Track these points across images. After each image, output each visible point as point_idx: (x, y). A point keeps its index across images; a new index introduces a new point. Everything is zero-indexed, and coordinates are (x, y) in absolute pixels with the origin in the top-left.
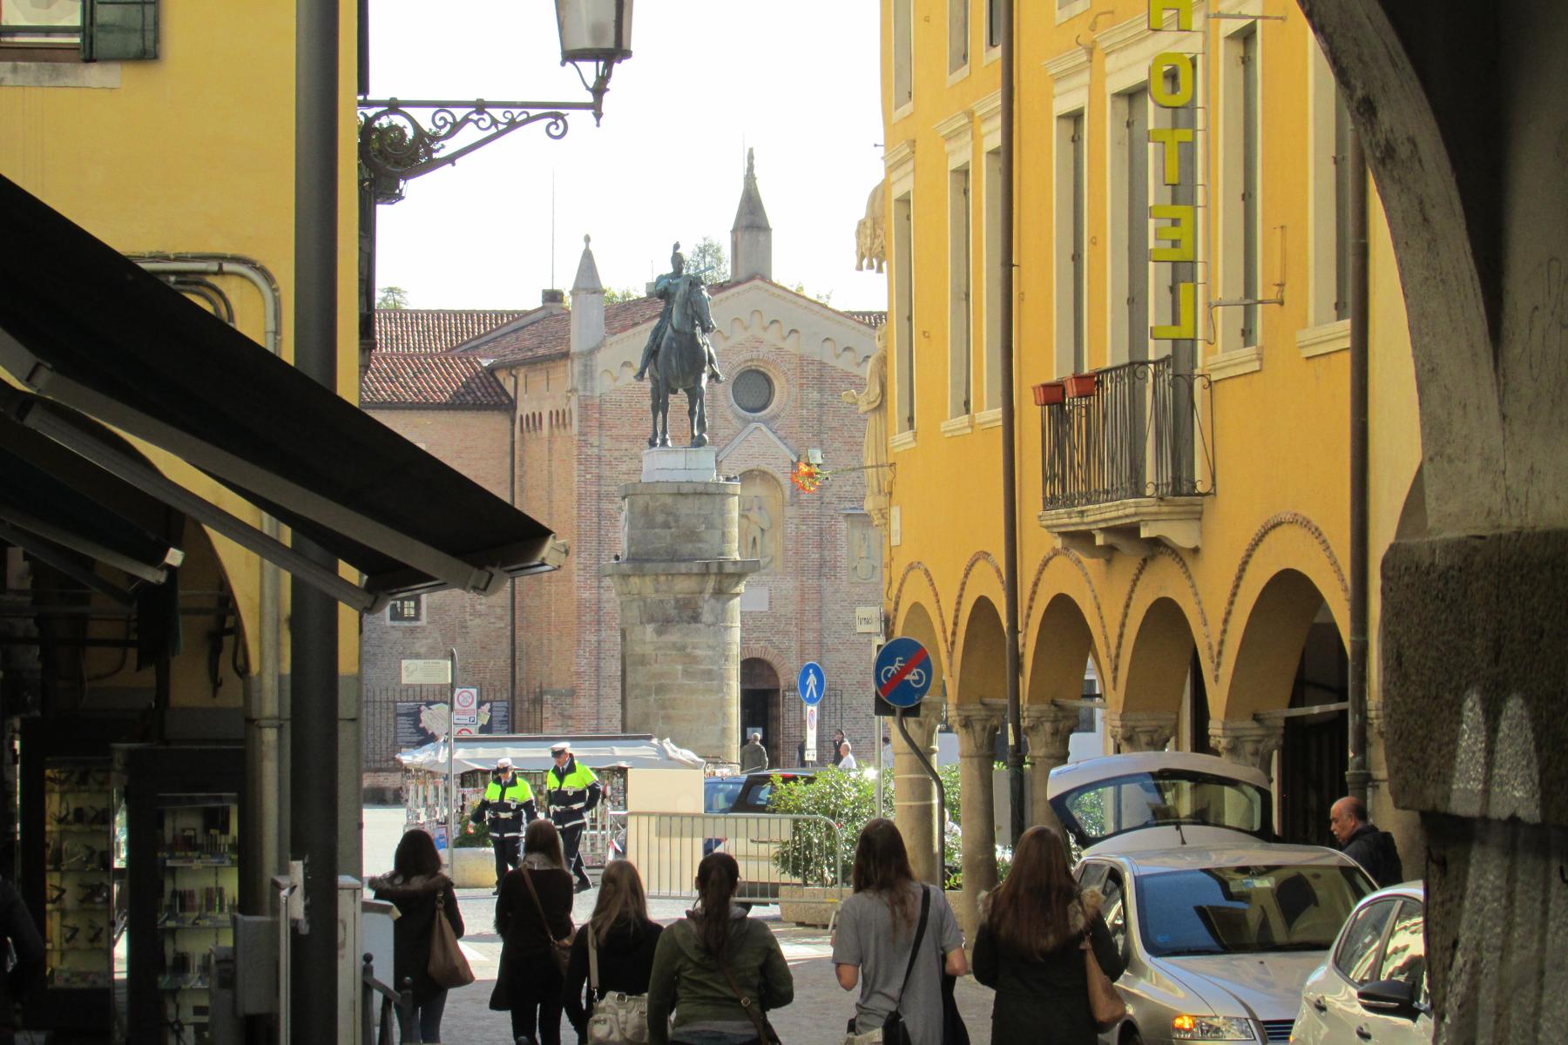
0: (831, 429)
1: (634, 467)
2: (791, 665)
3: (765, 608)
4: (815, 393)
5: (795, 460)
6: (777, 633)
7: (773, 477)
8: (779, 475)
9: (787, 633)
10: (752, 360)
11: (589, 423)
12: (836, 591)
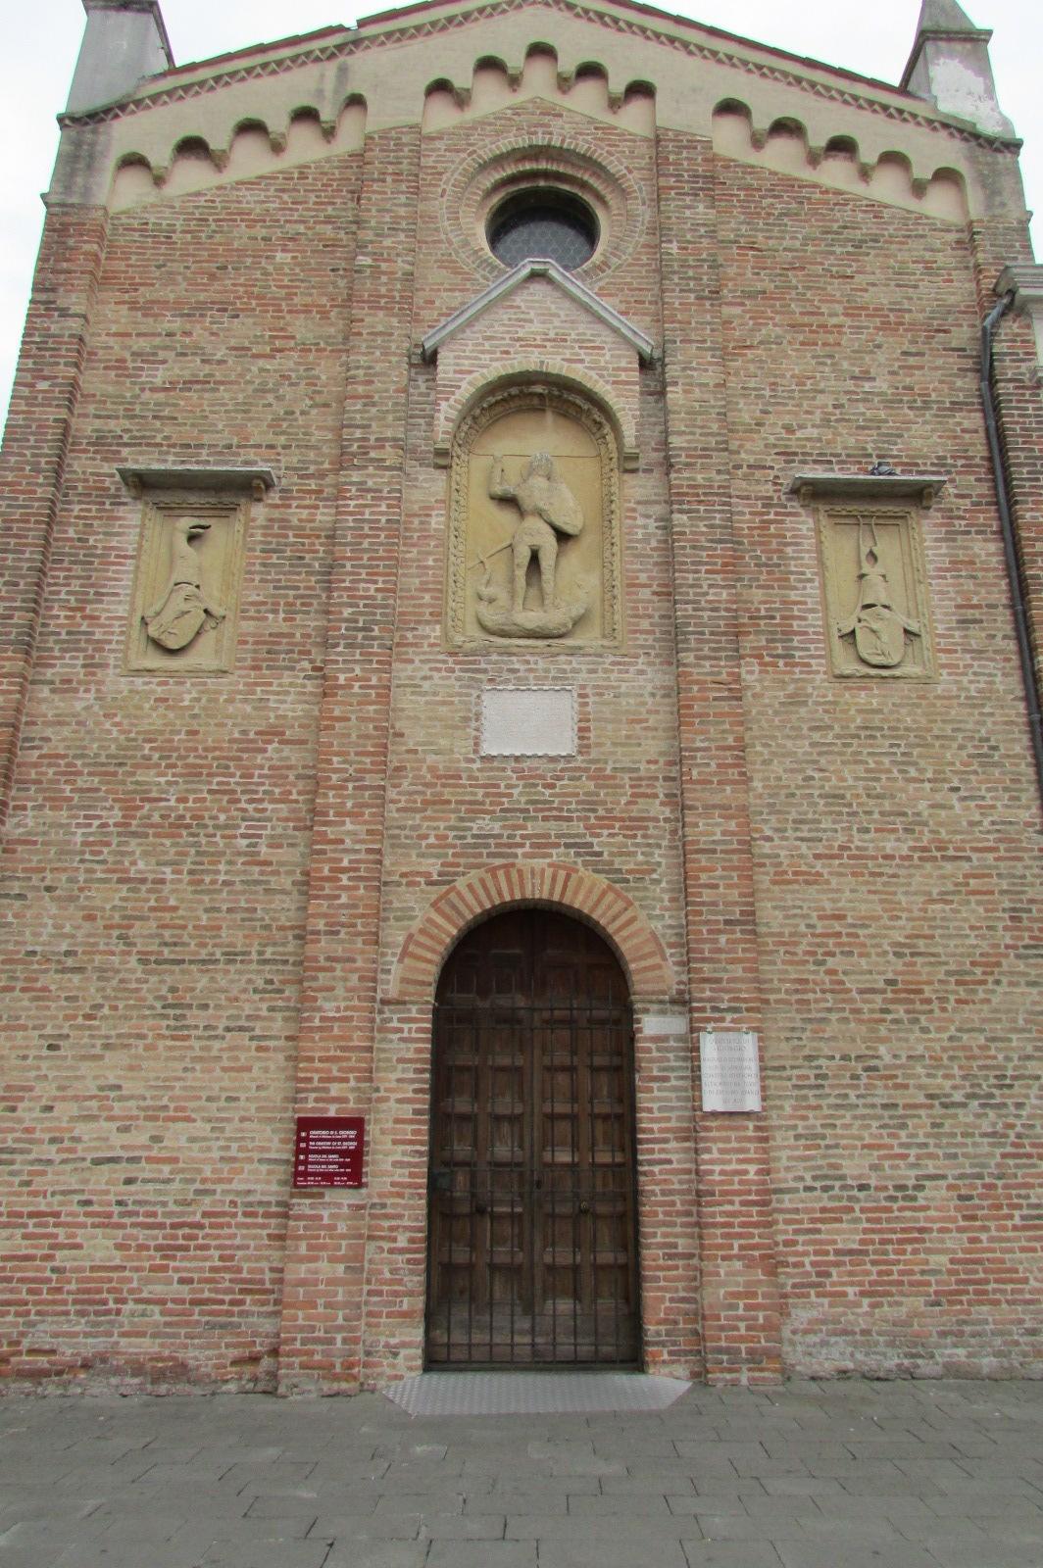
1: (187, 375)
2: (657, 926)
3: (565, 744)
4: (701, 208)
6: (607, 821)
9: (635, 824)
12: (796, 700)
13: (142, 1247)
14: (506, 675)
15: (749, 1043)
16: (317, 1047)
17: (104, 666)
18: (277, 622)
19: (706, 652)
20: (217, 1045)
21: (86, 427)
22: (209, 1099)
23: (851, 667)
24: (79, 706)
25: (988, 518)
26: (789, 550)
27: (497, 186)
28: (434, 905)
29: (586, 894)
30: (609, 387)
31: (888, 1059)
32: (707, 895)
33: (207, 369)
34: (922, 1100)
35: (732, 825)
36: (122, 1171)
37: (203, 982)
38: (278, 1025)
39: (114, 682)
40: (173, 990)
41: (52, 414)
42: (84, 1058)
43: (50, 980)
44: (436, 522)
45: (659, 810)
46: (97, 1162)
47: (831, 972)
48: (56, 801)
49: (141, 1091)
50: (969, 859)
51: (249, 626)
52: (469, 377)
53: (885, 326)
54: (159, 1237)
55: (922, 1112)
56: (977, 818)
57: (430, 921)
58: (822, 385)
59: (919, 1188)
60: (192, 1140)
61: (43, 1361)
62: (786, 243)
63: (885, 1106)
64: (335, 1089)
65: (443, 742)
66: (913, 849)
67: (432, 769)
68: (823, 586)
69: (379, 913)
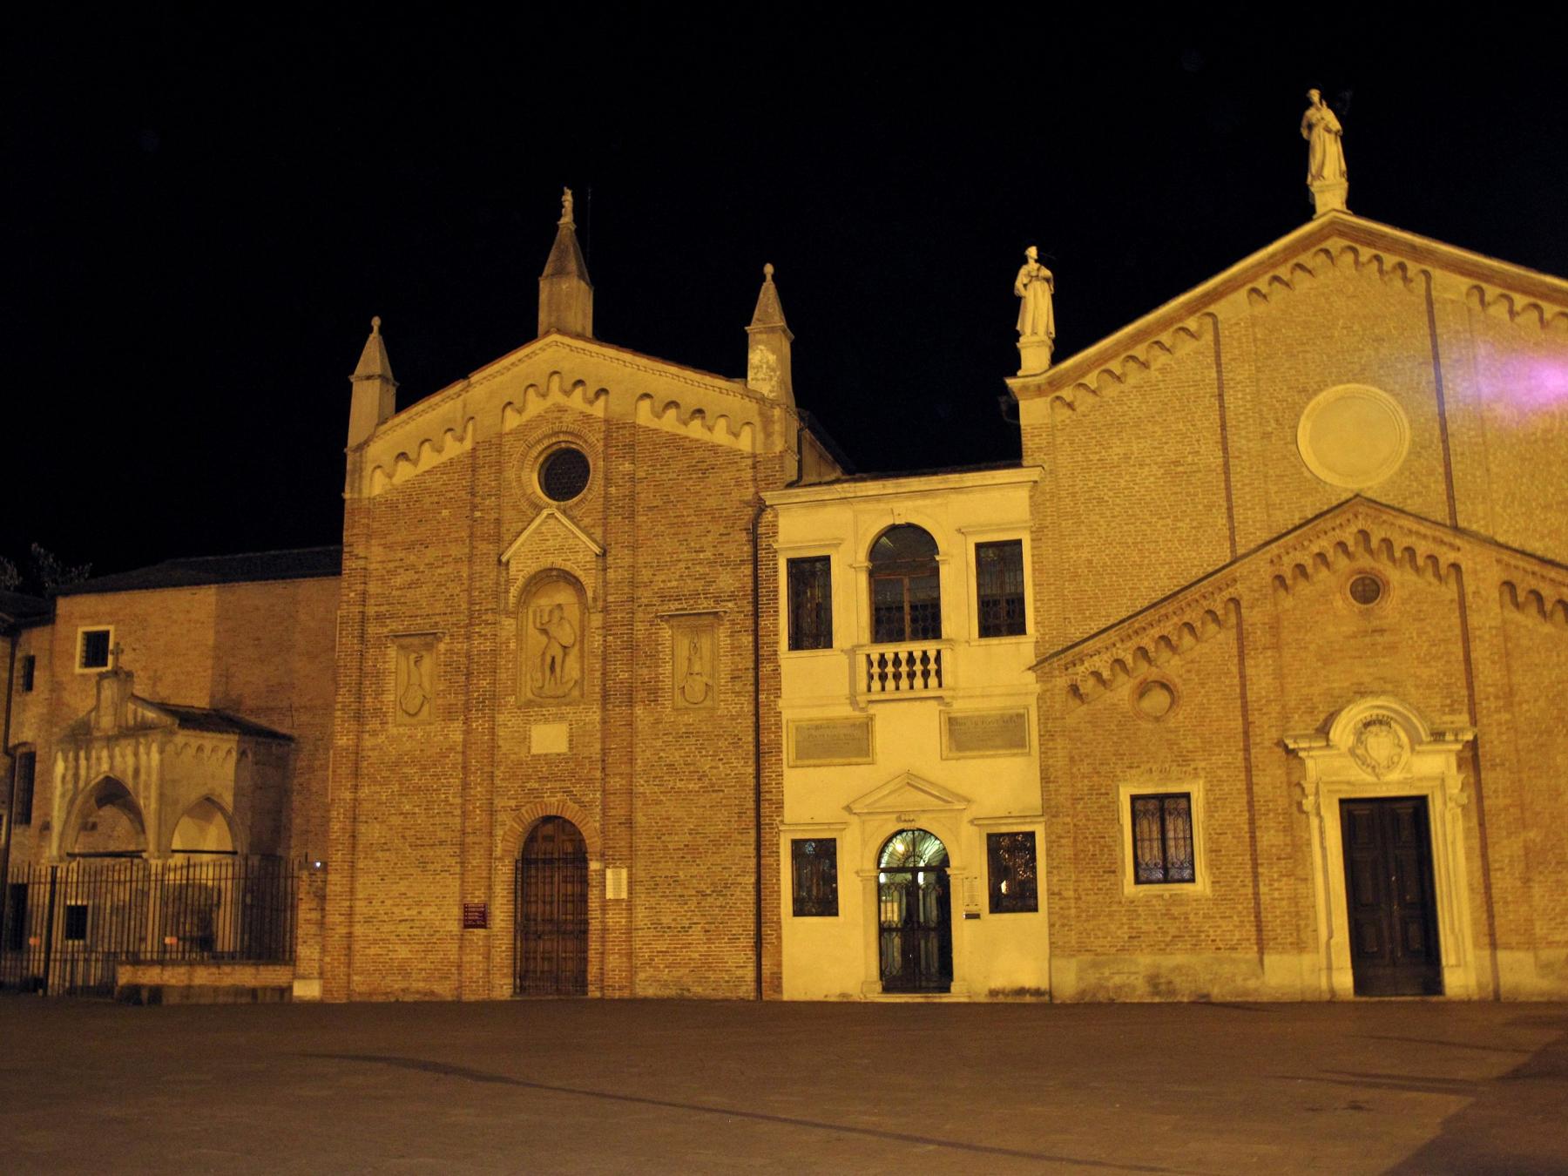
0: (651, 509)
3: (563, 747)
5: (598, 550)
6: (579, 781)
7: (577, 580)
8: (579, 573)
10: (556, 434)
11: (355, 531)
13: (417, 951)
14: (540, 717)
15: (624, 873)
16: (470, 878)
17: (386, 723)
18: (451, 699)
19: (617, 704)
20: (438, 877)
21: (371, 610)
22: (437, 897)
23: (681, 703)
24: (380, 741)
25: (749, 623)
26: (660, 647)
27: (540, 454)
28: (514, 819)
29: (571, 813)
30: (581, 573)
31: (682, 877)
32: (613, 812)
33: (416, 576)
34: (694, 893)
35: (624, 782)
36: (409, 924)
37: (432, 853)
38: (458, 869)
39: (393, 730)
40: (422, 856)
41: (357, 609)
42: (392, 883)
43: (379, 854)
44: (512, 646)
45: (598, 774)
46: (400, 921)
47: (663, 842)
48: (375, 782)
49: (412, 895)
50: (723, 791)
51: (440, 701)
52: (522, 573)
53: (714, 520)
54: (422, 947)
55: (694, 898)
56: (729, 772)
57: (512, 826)
58: (681, 556)
59: (690, 927)
60: (431, 912)
61: (389, 990)
62: (670, 476)
63: (680, 896)
64: (477, 893)
65: (516, 749)
66: (701, 787)
67: (512, 761)
68: (673, 665)
69: (492, 825)
